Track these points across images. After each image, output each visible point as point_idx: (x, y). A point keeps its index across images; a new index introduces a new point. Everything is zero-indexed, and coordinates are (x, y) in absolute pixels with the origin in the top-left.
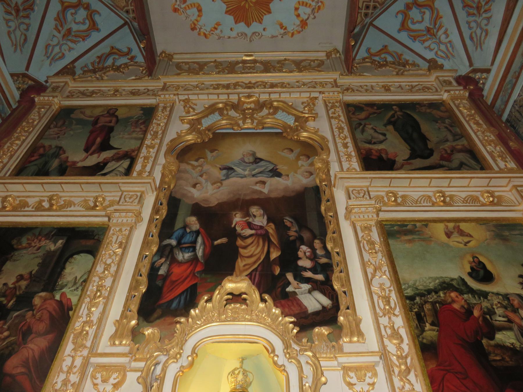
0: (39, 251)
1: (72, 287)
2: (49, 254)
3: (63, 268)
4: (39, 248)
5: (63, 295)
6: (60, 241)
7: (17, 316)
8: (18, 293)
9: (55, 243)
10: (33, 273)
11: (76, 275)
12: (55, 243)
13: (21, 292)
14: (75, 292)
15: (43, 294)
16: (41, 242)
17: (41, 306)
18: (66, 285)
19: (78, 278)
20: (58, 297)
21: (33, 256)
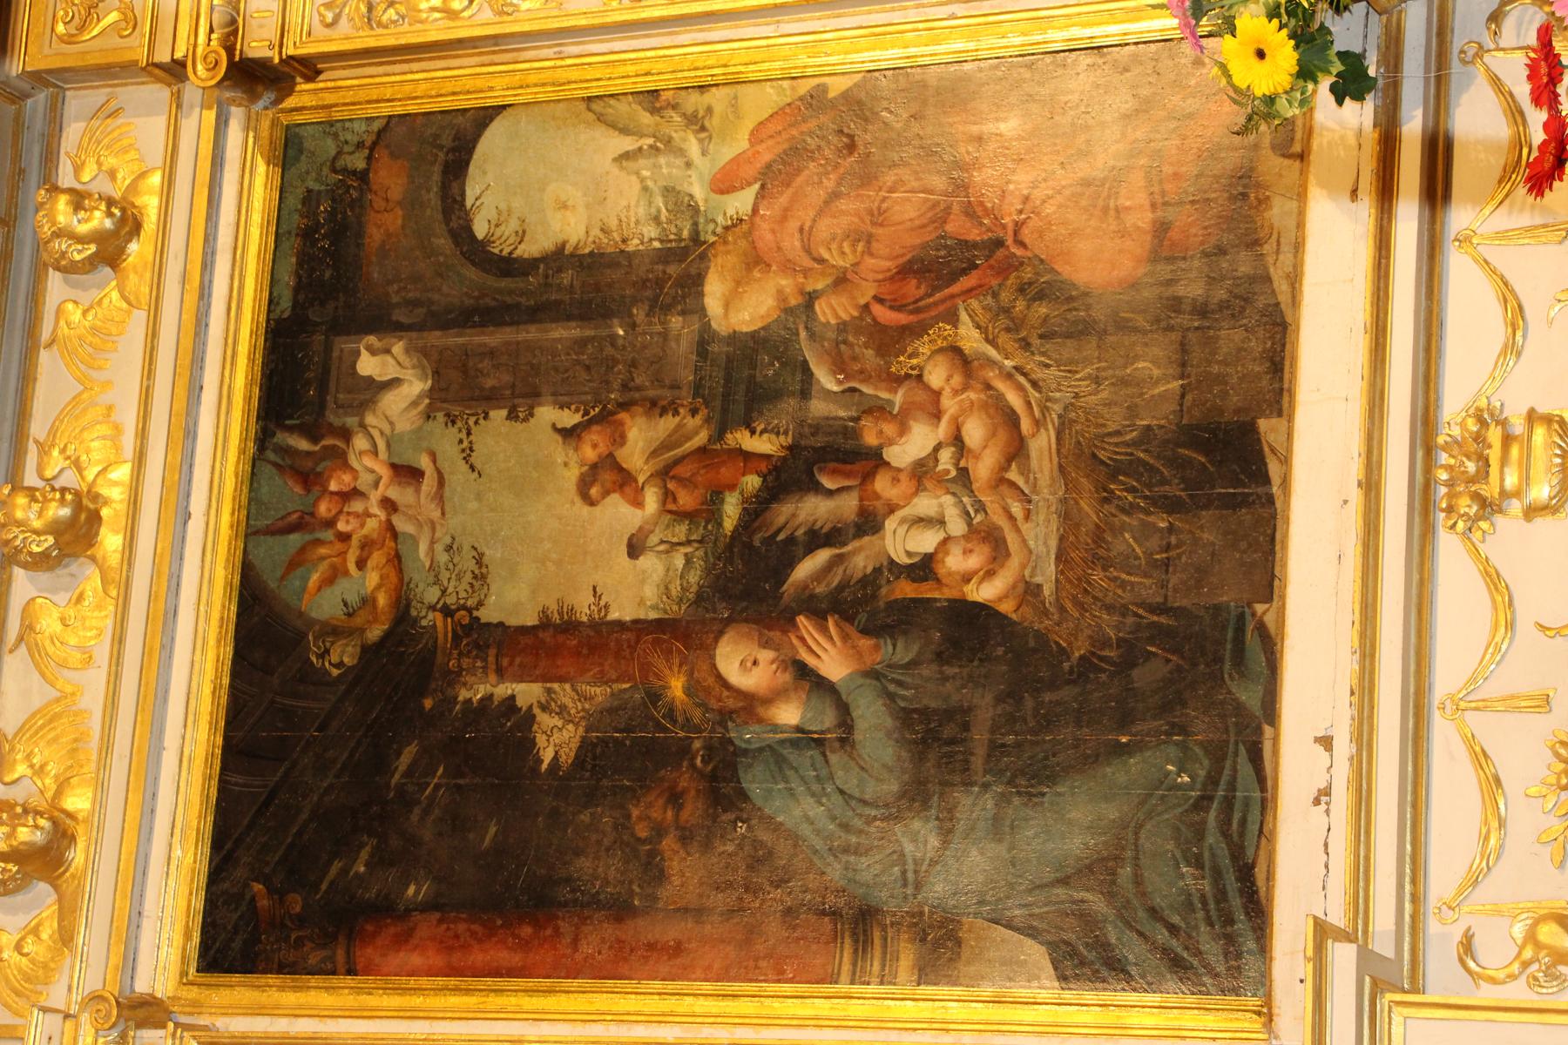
0: (424, 462)
1: (681, 152)
2: (460, 393)
3: (559, 258)
4: (407, 473)
5: (724, 184)
6: (368, 365)
7: (839, 365)
8: (701, 439)
9: (377, 388)
10: (569, 418)
11: (604, 162)
12: (377, 388)
13: (692, 422)
14: (714, 123)
15: (714, 291)
16: (364, 481)
17: (788, 267)
18: (668, 191)
19: (628, 144)
20: (740, 203)
21: (458, 475)
